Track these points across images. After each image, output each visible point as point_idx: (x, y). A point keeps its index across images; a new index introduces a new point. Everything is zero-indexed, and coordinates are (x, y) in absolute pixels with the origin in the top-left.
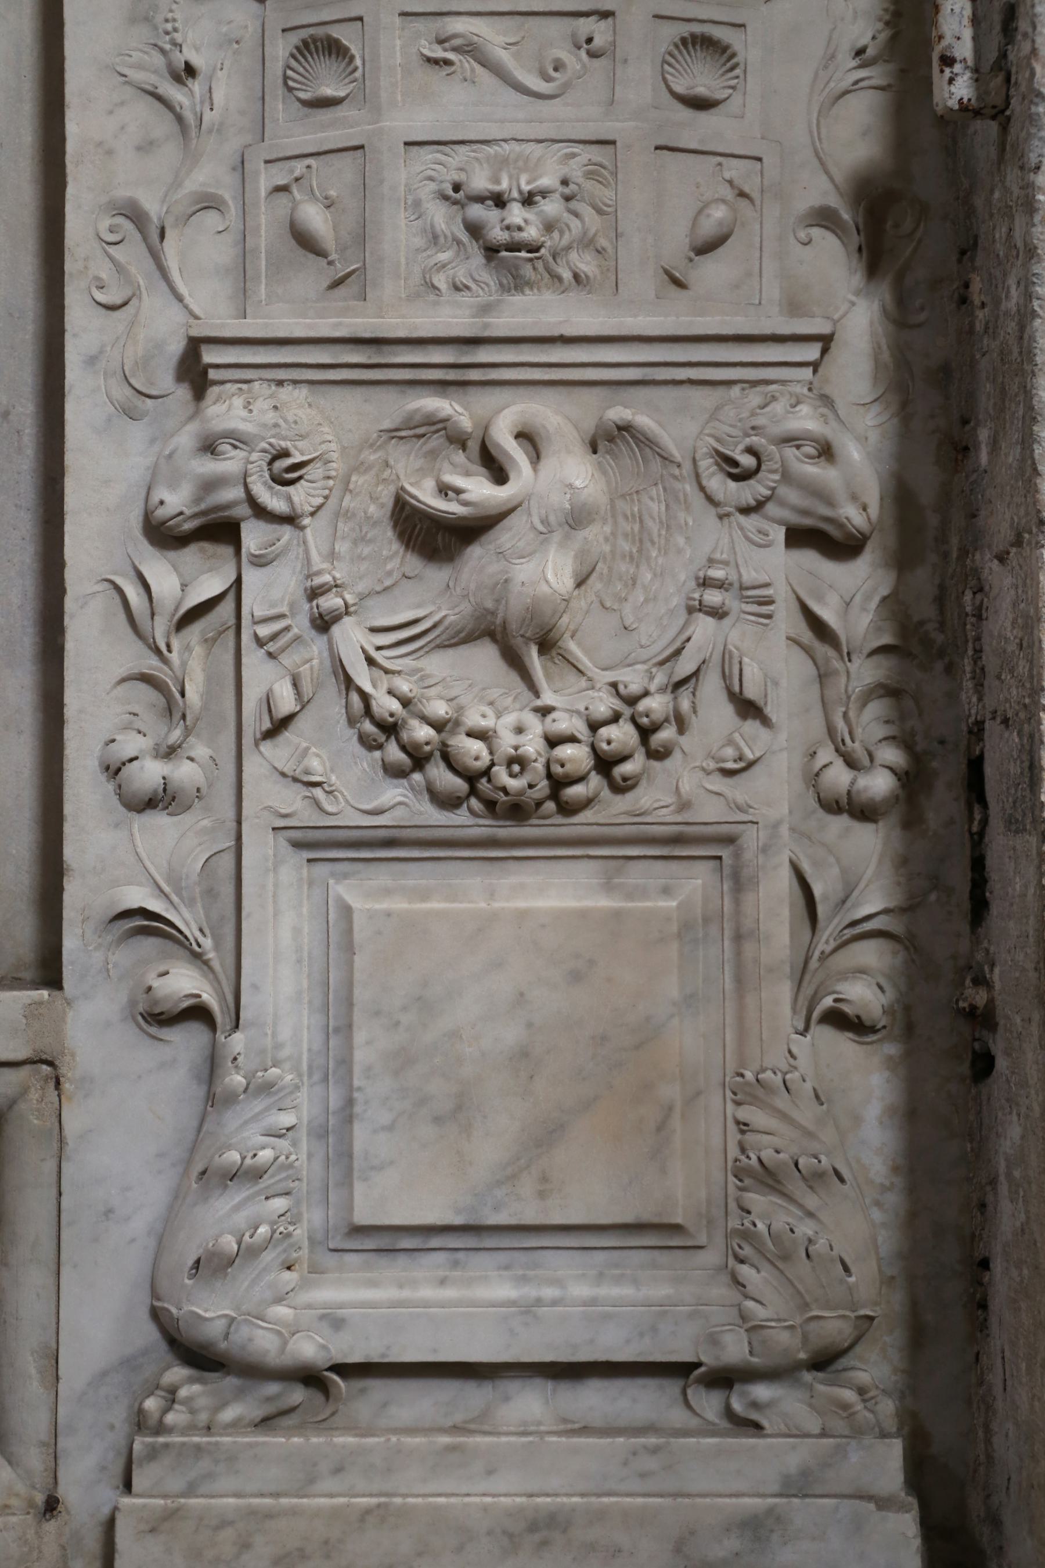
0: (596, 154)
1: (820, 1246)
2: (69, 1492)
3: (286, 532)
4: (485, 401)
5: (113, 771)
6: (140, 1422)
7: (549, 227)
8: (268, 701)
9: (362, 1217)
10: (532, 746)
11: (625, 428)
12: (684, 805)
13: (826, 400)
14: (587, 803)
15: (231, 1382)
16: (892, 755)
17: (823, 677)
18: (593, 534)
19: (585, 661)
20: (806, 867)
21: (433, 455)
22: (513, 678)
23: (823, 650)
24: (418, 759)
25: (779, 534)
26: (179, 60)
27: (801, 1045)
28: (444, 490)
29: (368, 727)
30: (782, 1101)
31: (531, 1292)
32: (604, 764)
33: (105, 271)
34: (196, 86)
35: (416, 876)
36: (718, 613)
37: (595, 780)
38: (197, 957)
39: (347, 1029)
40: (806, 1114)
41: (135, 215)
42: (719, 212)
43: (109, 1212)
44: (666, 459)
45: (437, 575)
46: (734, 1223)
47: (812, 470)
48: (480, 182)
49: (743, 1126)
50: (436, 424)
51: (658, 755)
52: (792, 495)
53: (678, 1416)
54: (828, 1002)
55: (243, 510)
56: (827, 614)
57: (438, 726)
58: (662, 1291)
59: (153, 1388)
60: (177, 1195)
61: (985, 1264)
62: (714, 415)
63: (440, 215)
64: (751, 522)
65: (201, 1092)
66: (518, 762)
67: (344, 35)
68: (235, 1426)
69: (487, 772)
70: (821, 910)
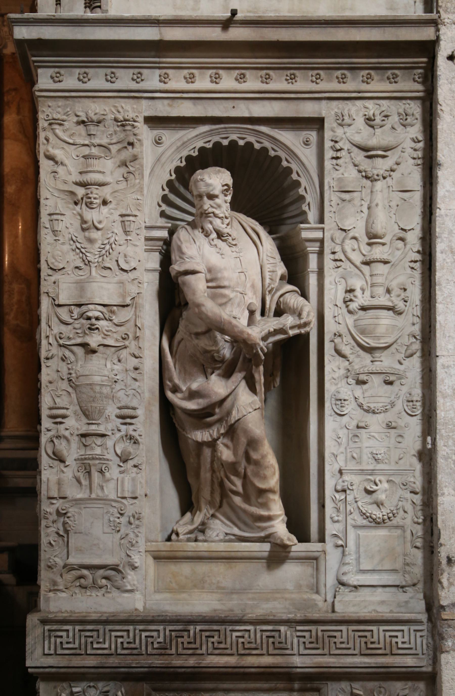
0: (388, 449)
1: (414, 572)
2: (328, 599)
3: (352, 491)
4: (375, 476)
5: (331, 518)
6: (336, 591)
7: (382, 457)
8: (350, 511)
9: (361, 569)
10: (381, 516)
11: (391, 480)
12: (398, 523)
13: (414, 477)
14: (387, 523)
15: (346, 587)
16: (422, 517)
17: (414, 508)
18: (388, 492)
19: (387, 507)
20: (412, 530)
21: (369, 483)
22: (378, 508)
23: (414, 505)
24: (367, 517)
25: (409, 492)
26: (339, 436)
27: (411, 550)
28: (371, 487)
29: (362, 514)
30: (409, 556)
31: (380, 577)
32: (389, 518)
33: (330, 460)
34: (341, 439)
35: (367, 531)
36: (402, 501)
37: (388, 520)
38: (341, 539)
39: (359, 548)
40: (412, 557)
41: (333, 454)
42: (402, 455)
43: (331, 568)
44: (396, 484)
45: (369, 496)
46: (404, 569)
47: (413, 485)
48: (375, 452)
49: (405, 559)
50: (369, 479)
51: (395, 517)
52: (410, 488)
53: (397, 591)
54: (414, 545)
55: (347, 489)
56: (415, 501)
57: (370, 513)
58: (395, 577)
59: (338, 587)
60: (339, 567)
61: (432, 575)
62: (401, 478)
63: (370, 456)
64: (406, 491)
65: (342, 555)
66: (379, 518)
67: (358, 435)
68: (347, 592)
69: (376, 519)
70: (414, 535)
